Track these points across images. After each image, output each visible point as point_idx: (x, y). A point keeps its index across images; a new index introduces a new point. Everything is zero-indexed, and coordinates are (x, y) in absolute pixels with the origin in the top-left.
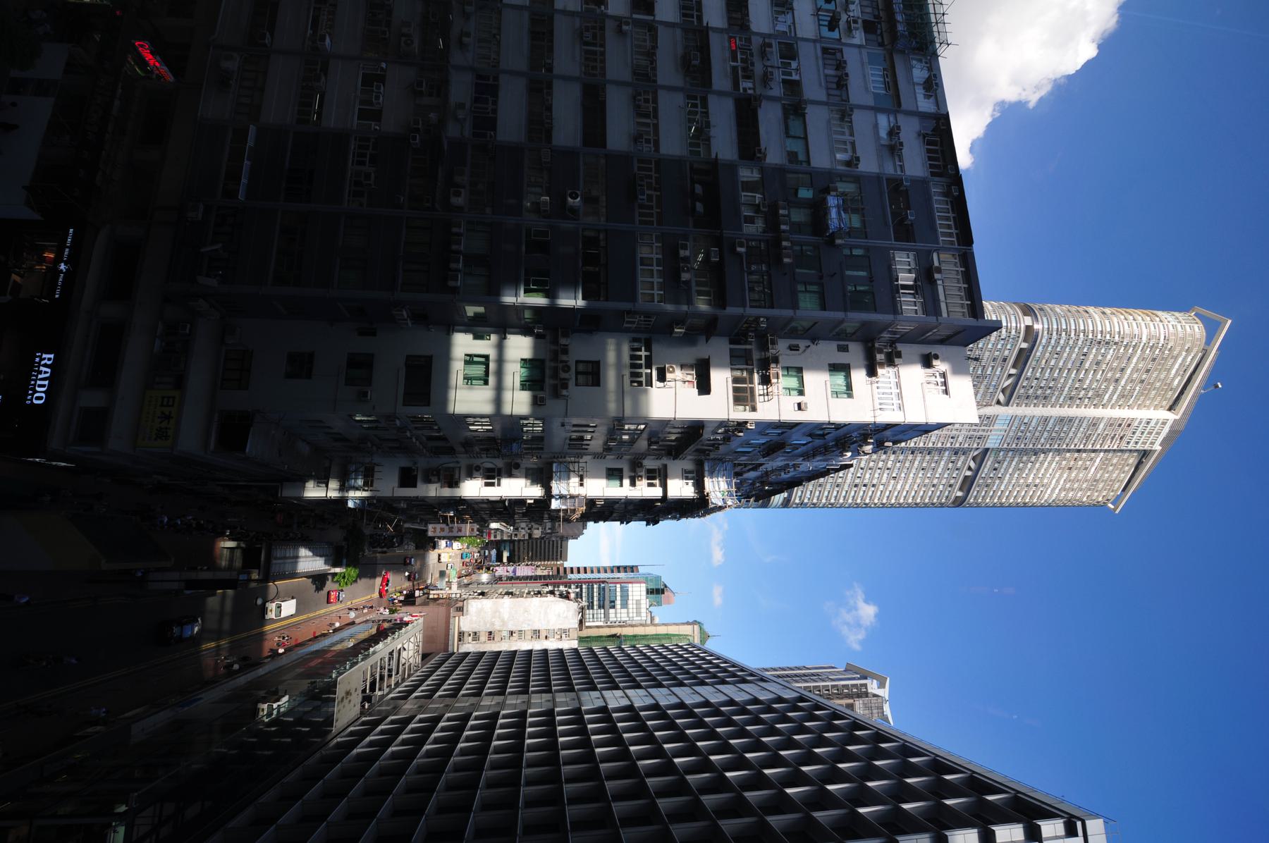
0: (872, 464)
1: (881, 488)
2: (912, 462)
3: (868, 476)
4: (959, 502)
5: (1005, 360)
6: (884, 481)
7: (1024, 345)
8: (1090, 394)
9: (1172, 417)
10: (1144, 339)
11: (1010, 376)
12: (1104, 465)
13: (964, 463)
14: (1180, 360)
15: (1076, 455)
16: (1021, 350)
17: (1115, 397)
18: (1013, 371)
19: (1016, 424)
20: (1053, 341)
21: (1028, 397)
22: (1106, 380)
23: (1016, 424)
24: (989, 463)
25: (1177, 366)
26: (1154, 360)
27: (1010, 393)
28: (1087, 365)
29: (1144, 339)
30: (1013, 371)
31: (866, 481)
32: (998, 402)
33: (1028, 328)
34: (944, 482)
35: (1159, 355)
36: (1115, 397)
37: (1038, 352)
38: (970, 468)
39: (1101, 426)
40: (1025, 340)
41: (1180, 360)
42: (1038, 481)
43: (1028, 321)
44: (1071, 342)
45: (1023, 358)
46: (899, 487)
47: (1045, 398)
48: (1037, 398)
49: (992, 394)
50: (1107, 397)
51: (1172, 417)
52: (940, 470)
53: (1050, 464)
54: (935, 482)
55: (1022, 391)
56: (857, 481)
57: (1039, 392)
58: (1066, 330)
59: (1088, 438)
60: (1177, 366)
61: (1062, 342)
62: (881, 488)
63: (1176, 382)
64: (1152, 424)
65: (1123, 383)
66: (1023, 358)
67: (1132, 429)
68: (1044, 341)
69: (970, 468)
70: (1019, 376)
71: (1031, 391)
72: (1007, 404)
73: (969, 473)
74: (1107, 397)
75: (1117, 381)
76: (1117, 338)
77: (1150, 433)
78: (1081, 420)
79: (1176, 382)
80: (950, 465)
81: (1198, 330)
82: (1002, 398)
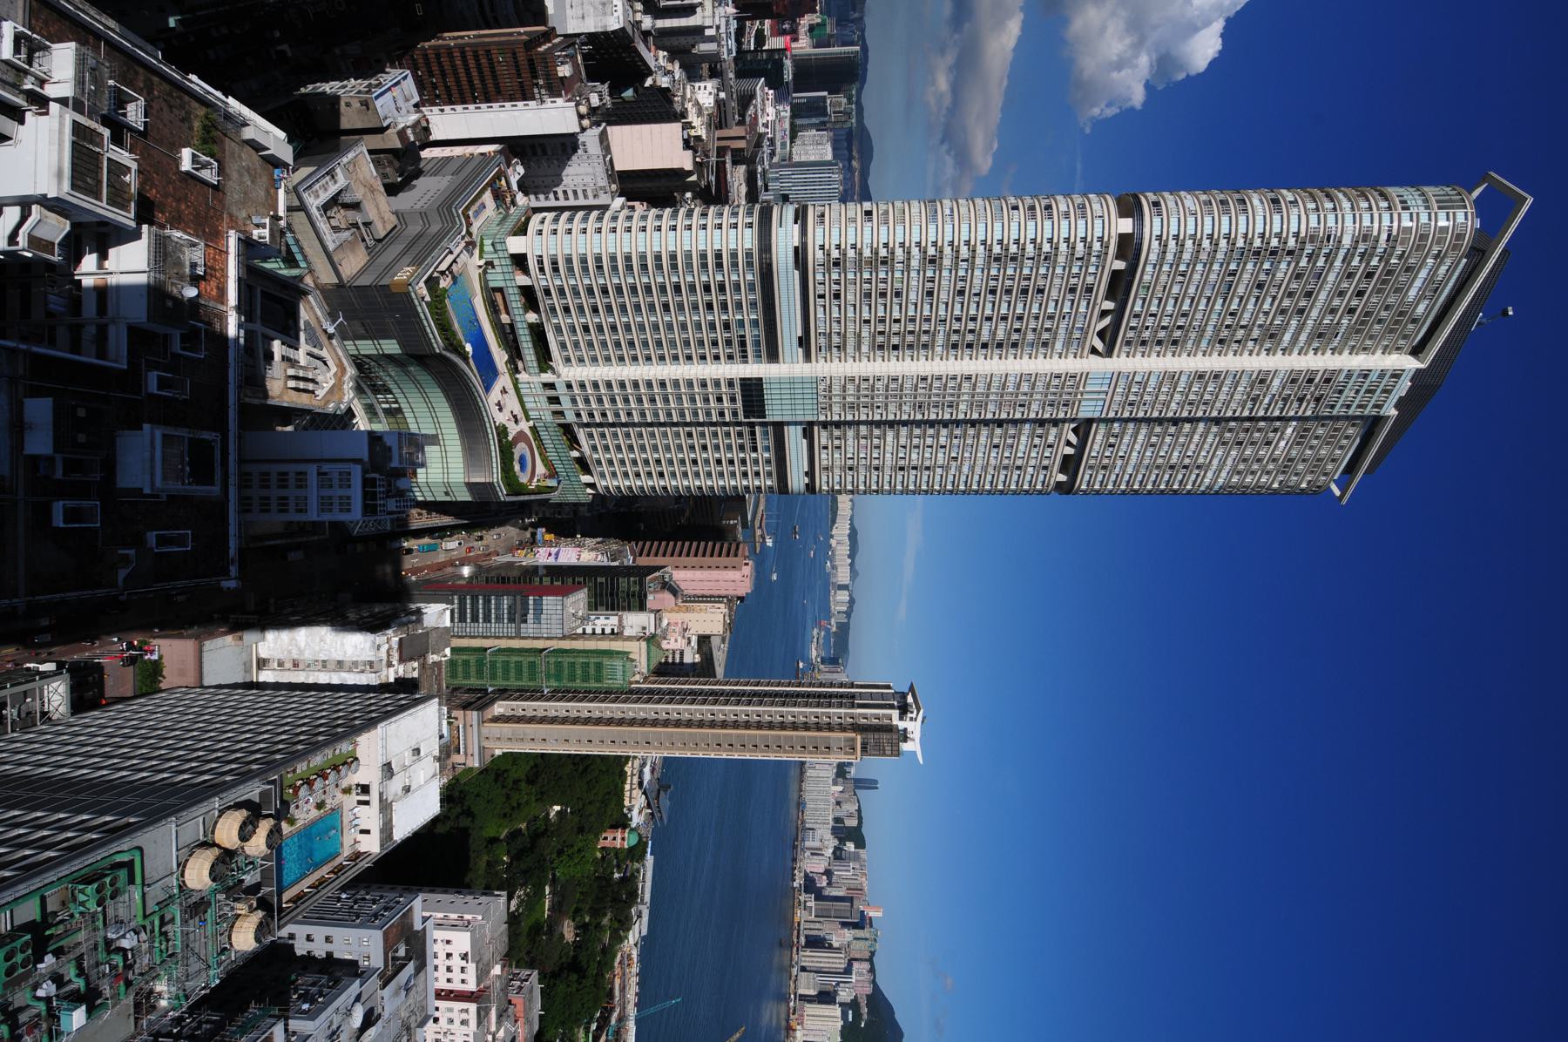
0: (916, 441)
1: (939, 471)
2: (978, 436)
3: (914, 456)
4: (1065, 489)
5: (1089, 290)
6: (940, 462)
7: (1120, 265)
8: (1256, 333)
9: (1411, 364)
10: (1347, 241)
11: (1104, 314)
12: (1300, 439)
13: (1059, 436)
14: (1423, 274)
15: (1247, 424)
16: (1115, 274)
17: (1303, 337)
18: (1109, 305)
19: (1122, 383)
20: (1169, 257)
21: (1144, 343)
22: (1283, 312)
23: (1122, 383)
24: (1098, 436)
25: (1418, 283)
26: (1370, 275)
27: (1109, 339)
28: (1241, 290)
29: (1347, 241)
30: (1109, 305)
31: (914, 463)
32: (1094, 351)
33: (1123, 238)
34: (1032, 462)
35: (1380, 269)
36: (1303, 337)
37: (1146, 273)
38: (1069, 443)
39: (1276, 383)
40: (1119, 256)
41: (1423, 274)
42: (1187, 461)
43: (1126, 226)
44: (1203, 256)
45: (1120, 286)
46: (965, 470)
47: (1175, 343)
48: (1159, 343)
49: (1081, 342)
50: (1287, 337)
51: (1411, 364)
52: (1022, 448)
53: (1204, 436)
54: (1019, 463)
55: (1131, 334)
56: (901, 463)
57: (1162, 334)
58: (1227, 237)
59: (1254, 400)
60: (1418, 283)
61: (1186, 256)
62: (939, 471)
63: (1421, 309)
64: (1373, 377)
65: (1314, 314)
66: (1120, 286)
67: (1334, 385)
68: (1153, 257)
69: (1069, 443)
70: (1118, 314)
71: (1146, 334)
72: (1109, 352)
73: (1069, 451)
74: (1287, 337)
75: (1301, 311)
76: (1292, 242)
77: (1368, 391)
78: (1237, 377)
79: (1421, 309)
80: (1037, 441)
81: (1464, 219)
82: (1099, 345)
